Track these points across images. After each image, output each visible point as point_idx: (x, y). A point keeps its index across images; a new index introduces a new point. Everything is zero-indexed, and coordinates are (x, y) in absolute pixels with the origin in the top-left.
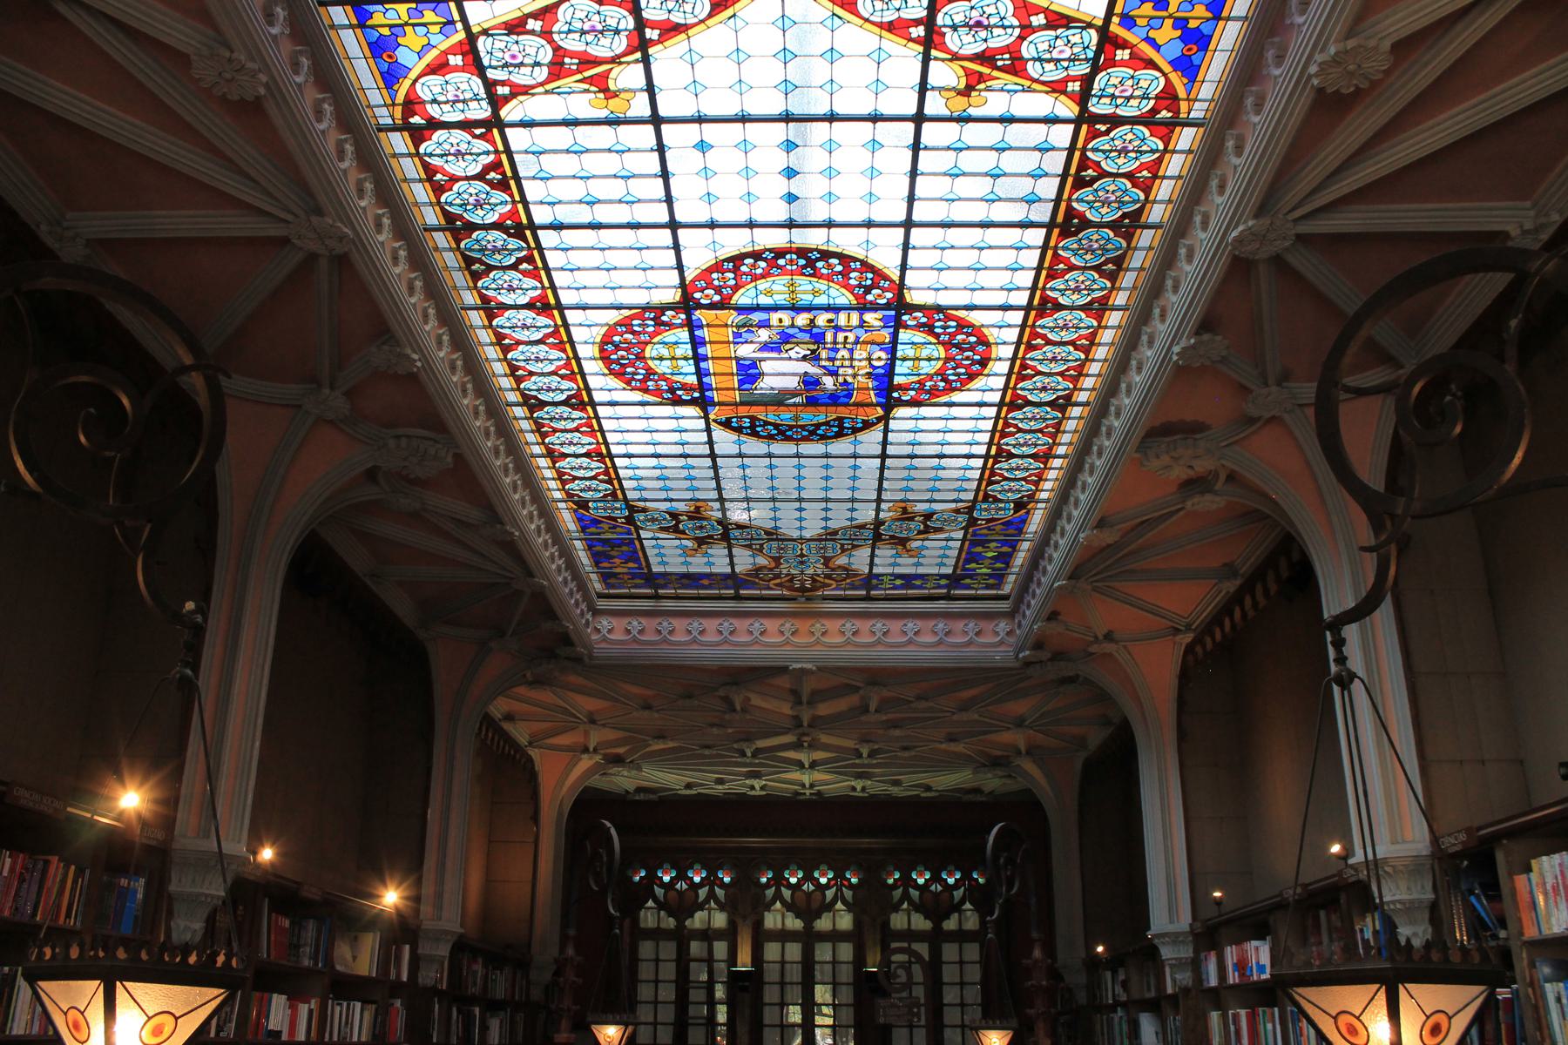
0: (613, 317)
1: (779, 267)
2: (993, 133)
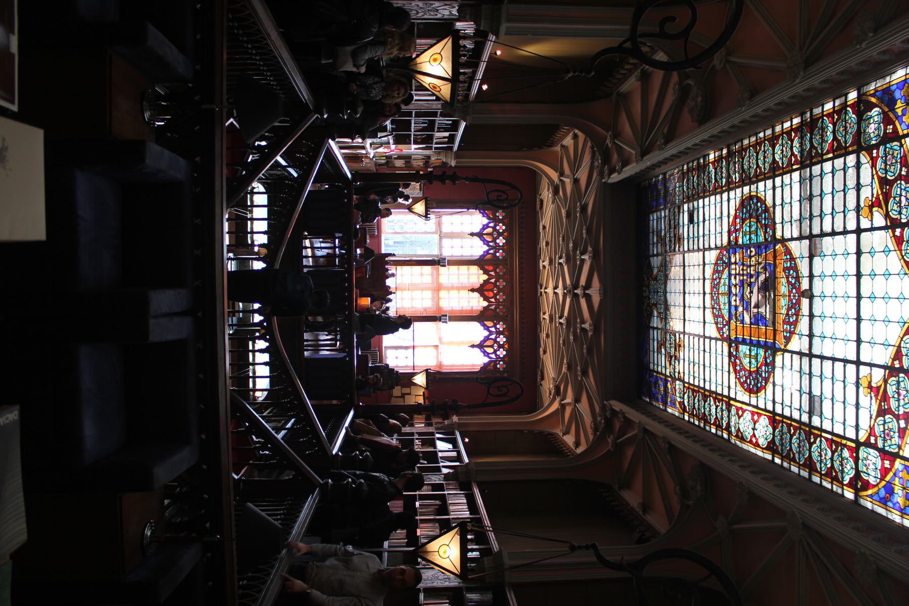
0: (769, 202)
1: (792, 289)
2: (851, 399)
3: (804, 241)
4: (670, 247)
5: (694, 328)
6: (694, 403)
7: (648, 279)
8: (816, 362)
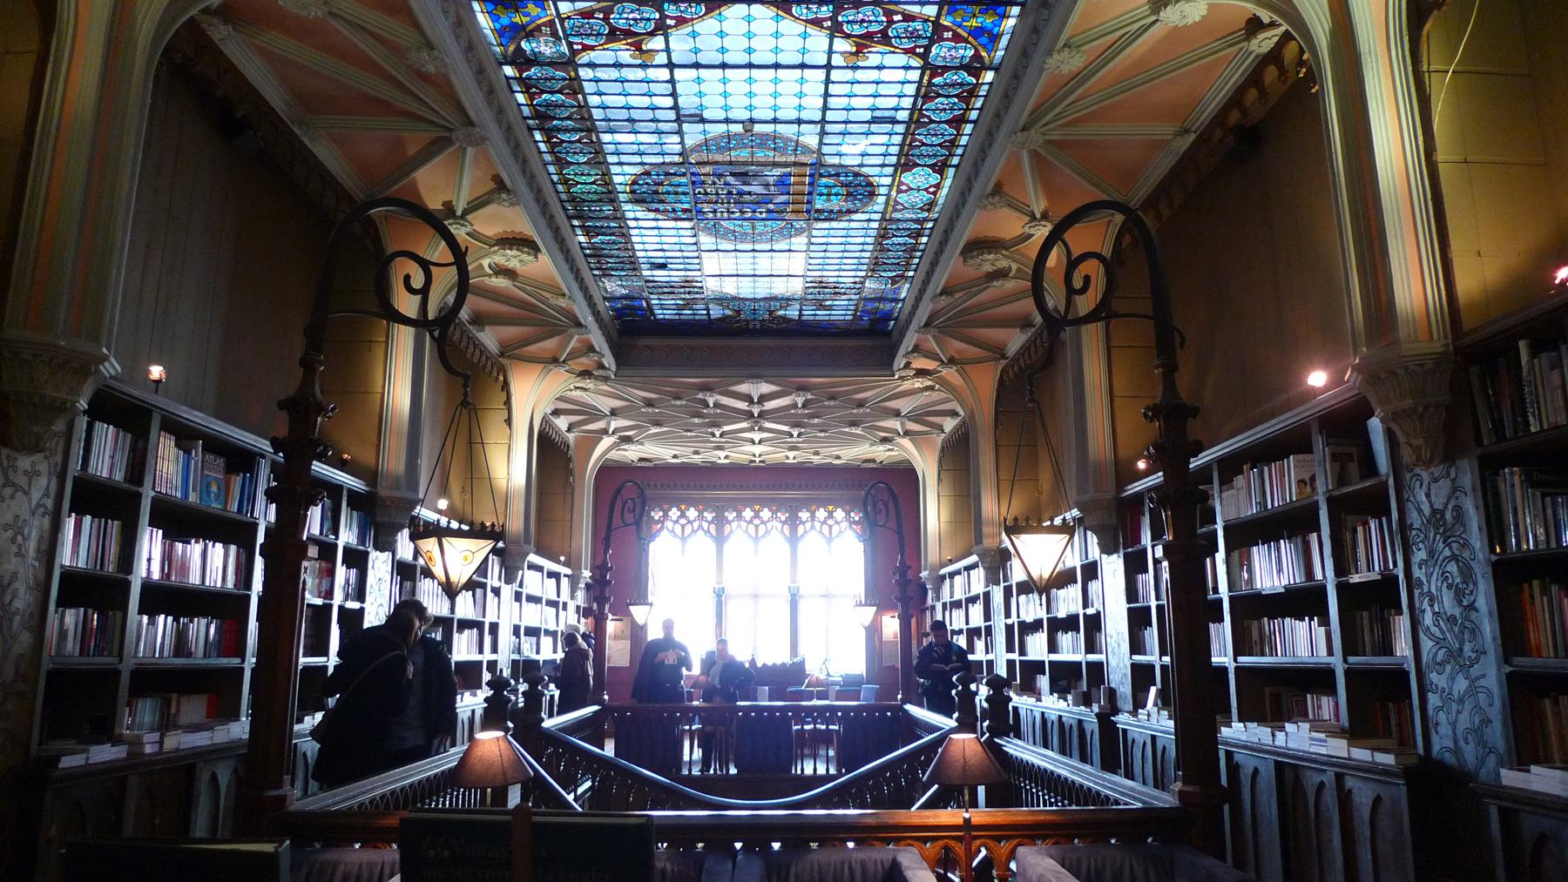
2: (873, 75)
3: (684, 129)
4: (697, 293)
5: (797, 264)
6: (892, 264)
7: (738, 322)
8: (830, 116)
